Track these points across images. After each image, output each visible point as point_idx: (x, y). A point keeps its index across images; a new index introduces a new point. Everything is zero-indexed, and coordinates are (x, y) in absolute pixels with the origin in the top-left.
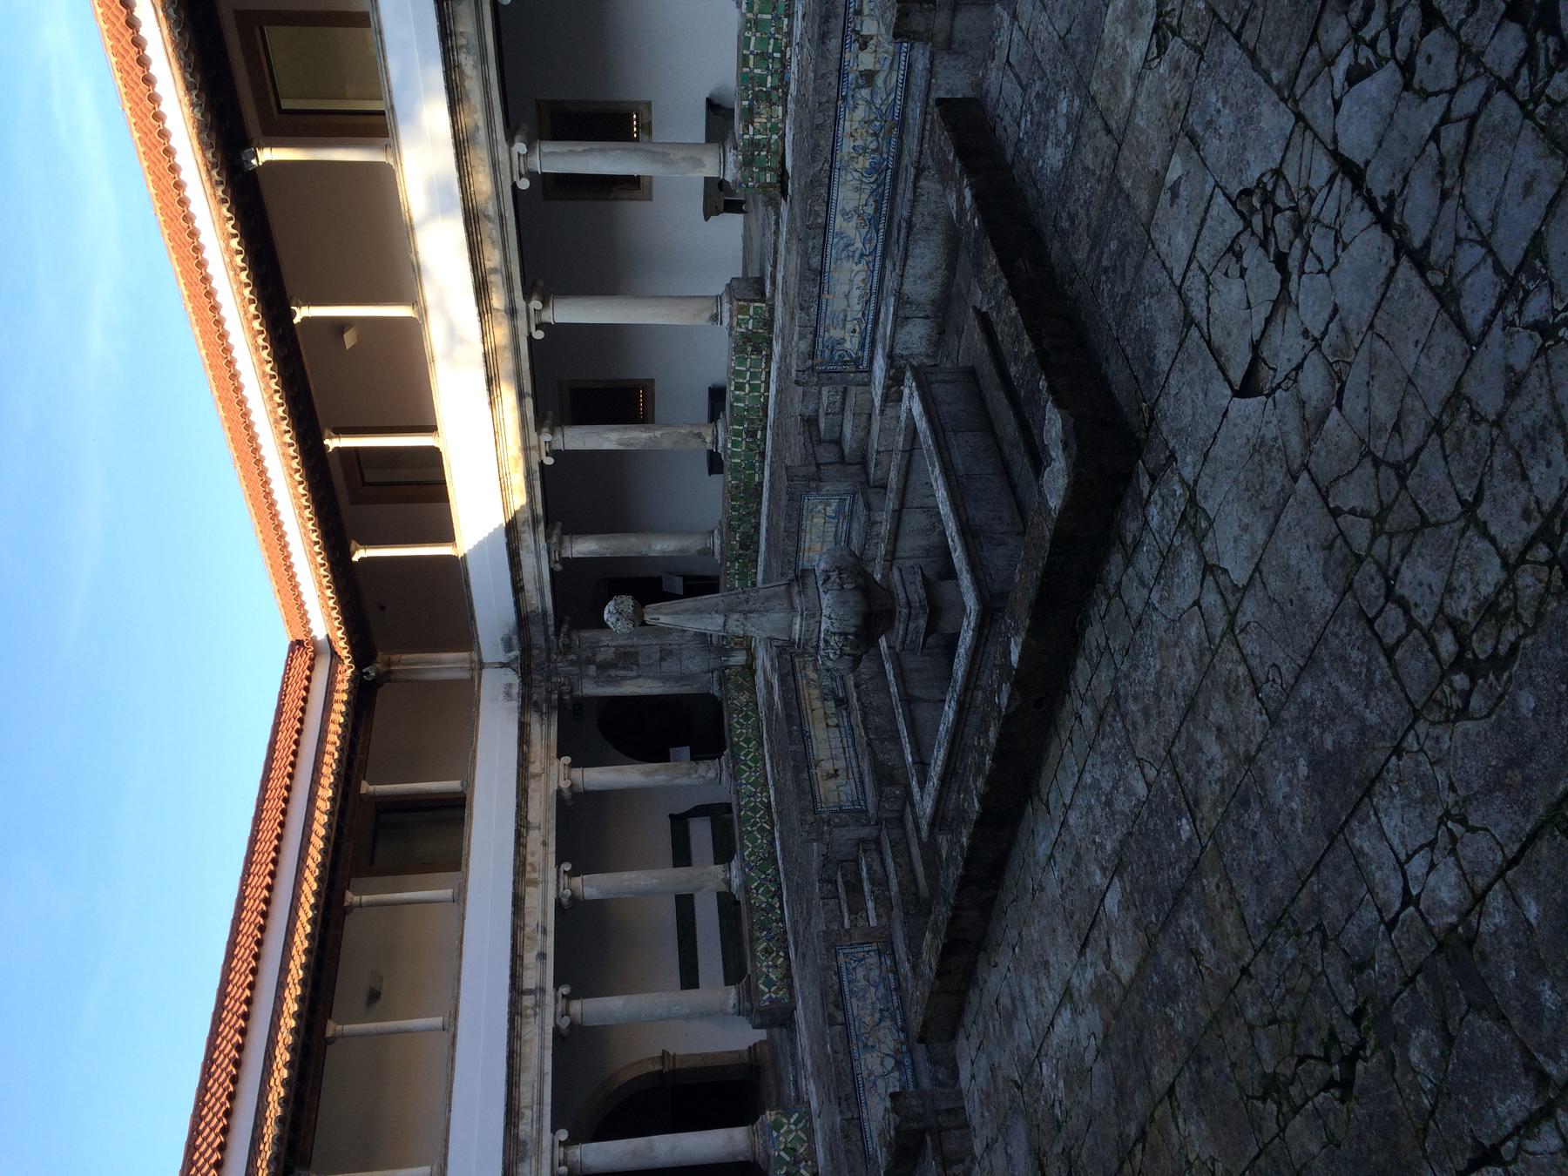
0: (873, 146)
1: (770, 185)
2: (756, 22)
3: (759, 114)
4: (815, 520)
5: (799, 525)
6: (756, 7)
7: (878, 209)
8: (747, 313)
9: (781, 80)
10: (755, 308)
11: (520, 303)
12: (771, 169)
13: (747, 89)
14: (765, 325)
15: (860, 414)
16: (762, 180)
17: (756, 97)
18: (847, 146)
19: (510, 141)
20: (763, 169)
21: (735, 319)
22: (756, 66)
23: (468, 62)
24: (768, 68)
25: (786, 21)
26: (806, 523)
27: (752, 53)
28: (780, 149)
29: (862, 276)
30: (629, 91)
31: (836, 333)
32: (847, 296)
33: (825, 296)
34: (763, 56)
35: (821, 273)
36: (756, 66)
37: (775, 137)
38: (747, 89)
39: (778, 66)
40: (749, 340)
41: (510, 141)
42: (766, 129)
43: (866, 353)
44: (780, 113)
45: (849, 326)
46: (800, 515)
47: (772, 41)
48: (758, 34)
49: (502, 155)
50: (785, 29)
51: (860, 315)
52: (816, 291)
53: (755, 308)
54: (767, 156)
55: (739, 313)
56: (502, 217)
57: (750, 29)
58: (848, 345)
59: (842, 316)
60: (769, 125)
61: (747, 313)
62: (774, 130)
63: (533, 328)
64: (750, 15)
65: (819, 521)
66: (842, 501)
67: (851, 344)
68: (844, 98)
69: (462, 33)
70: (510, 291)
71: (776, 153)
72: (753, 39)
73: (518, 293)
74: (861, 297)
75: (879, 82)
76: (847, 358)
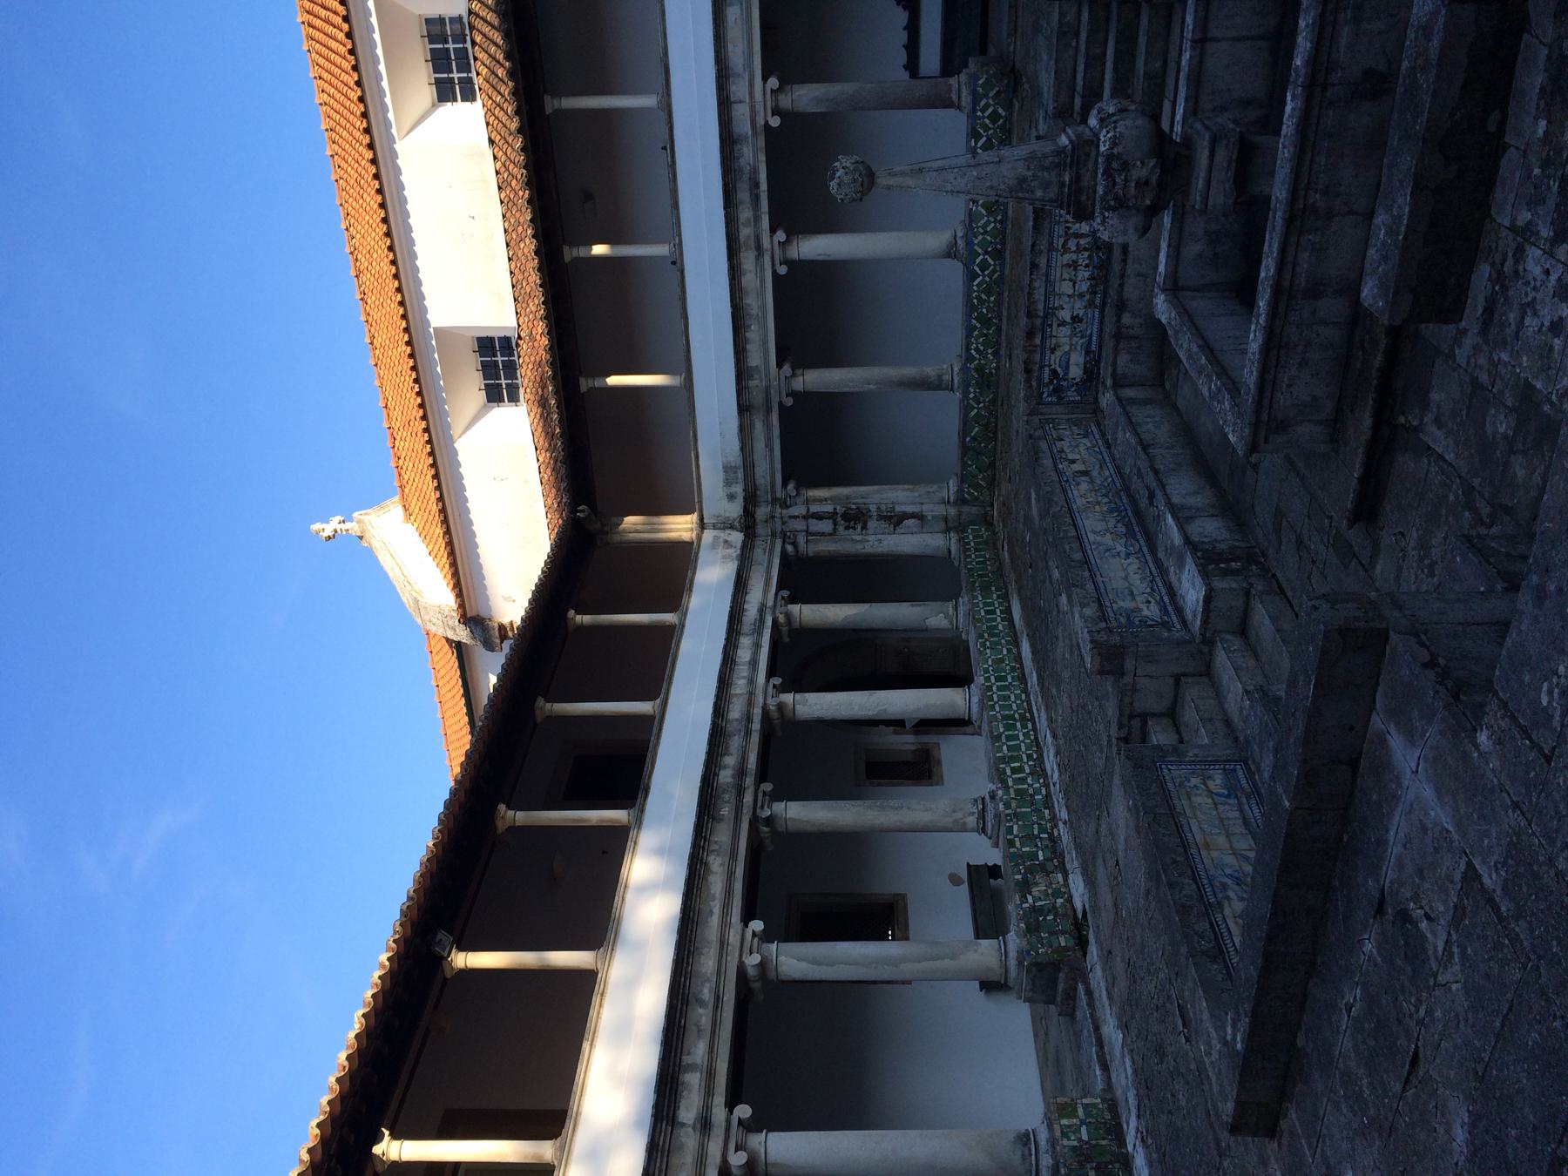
0: (1106, 500)
1: (1066, 949)
2: (1015, 814)
3: (1036, 884)
4: (1196, 800)
5: (1172, 808)
6: (1014, 805)
7: (1128, 526)
8: (1074, 1114)
9: (1054, 852)
10: (1086, 1106)
11: (719, 1113)
12: (1063, 932)
13: (1017, 865)
14: (1108, 1132)
15: (1211, 720)
16: (1055, 945)
17: (1030, 870)
18: (1080, 502)
19: (746, 919)
20: (1053, 933)
21: (1057, 1127)
22: (1022, 846)
23: (717, 864)
24: (1037, 846)
25: (1047, 812)
26: (1181, 804)
27: (1016, 836)
28: (1070, 912)
29: (1134, 567)
30: (883, 886)
31: (1128, 604)
32: (1126, 578)
33: (1099, 579)
34: (1030, 838)
35: (1086, 562)
36: (1022, 846)
37: (1060, 901)
38: (1017, 865)
39: (1047, 843)
40: (1089, 1159)
41: (746, 919)
42: (1047, 895)
43: (1174, 618)
44: (1061, 880)
45: (1139, 599)
46: (1167, 798)
47: (1036, 826)
48: (1020, 823)
49: (734, 937)
50: (1047, 817)
51: (1148, 590)
52: (1087, 574)
53: (1086, 1106)
54: (1055, 920)
55: (1061, 1116)
56: (718, 999)
57: (1011, 820)
58: (1146, 612)
59: (1126, 592)
60: (1050, 891)
61: (1074, 1114)
62: (1061, 895)
63: (732, 1147)
64: (1007, 812)
65: (1202, 800)
66: (1229, 774)
67: (1151, 611)
68: (1067, 481)
69: (716, 842)
70: (709, 1092)
71: (1065, 915)
72: (1015, 828)
73: (719, 1099)
74: (1142, 579)
75: (1095, 473)
76: (1149, 623)
